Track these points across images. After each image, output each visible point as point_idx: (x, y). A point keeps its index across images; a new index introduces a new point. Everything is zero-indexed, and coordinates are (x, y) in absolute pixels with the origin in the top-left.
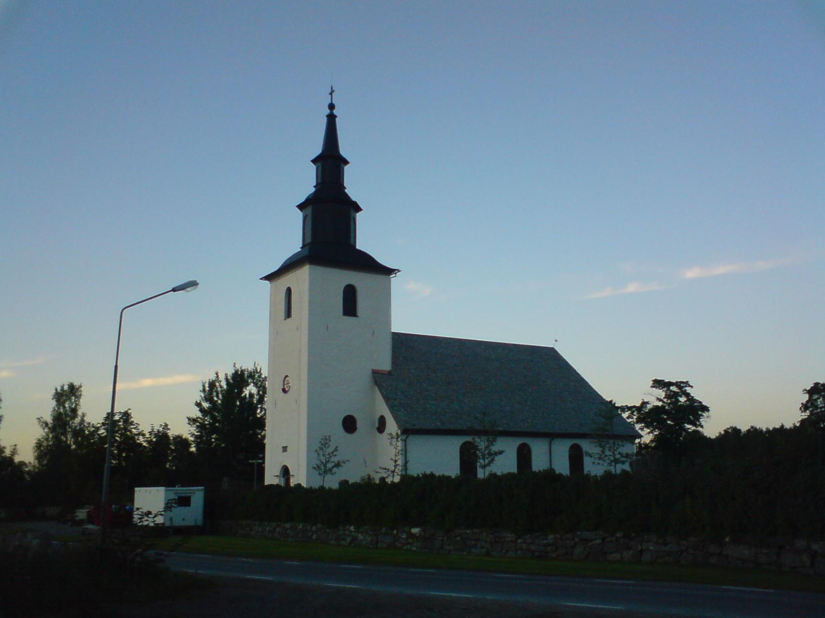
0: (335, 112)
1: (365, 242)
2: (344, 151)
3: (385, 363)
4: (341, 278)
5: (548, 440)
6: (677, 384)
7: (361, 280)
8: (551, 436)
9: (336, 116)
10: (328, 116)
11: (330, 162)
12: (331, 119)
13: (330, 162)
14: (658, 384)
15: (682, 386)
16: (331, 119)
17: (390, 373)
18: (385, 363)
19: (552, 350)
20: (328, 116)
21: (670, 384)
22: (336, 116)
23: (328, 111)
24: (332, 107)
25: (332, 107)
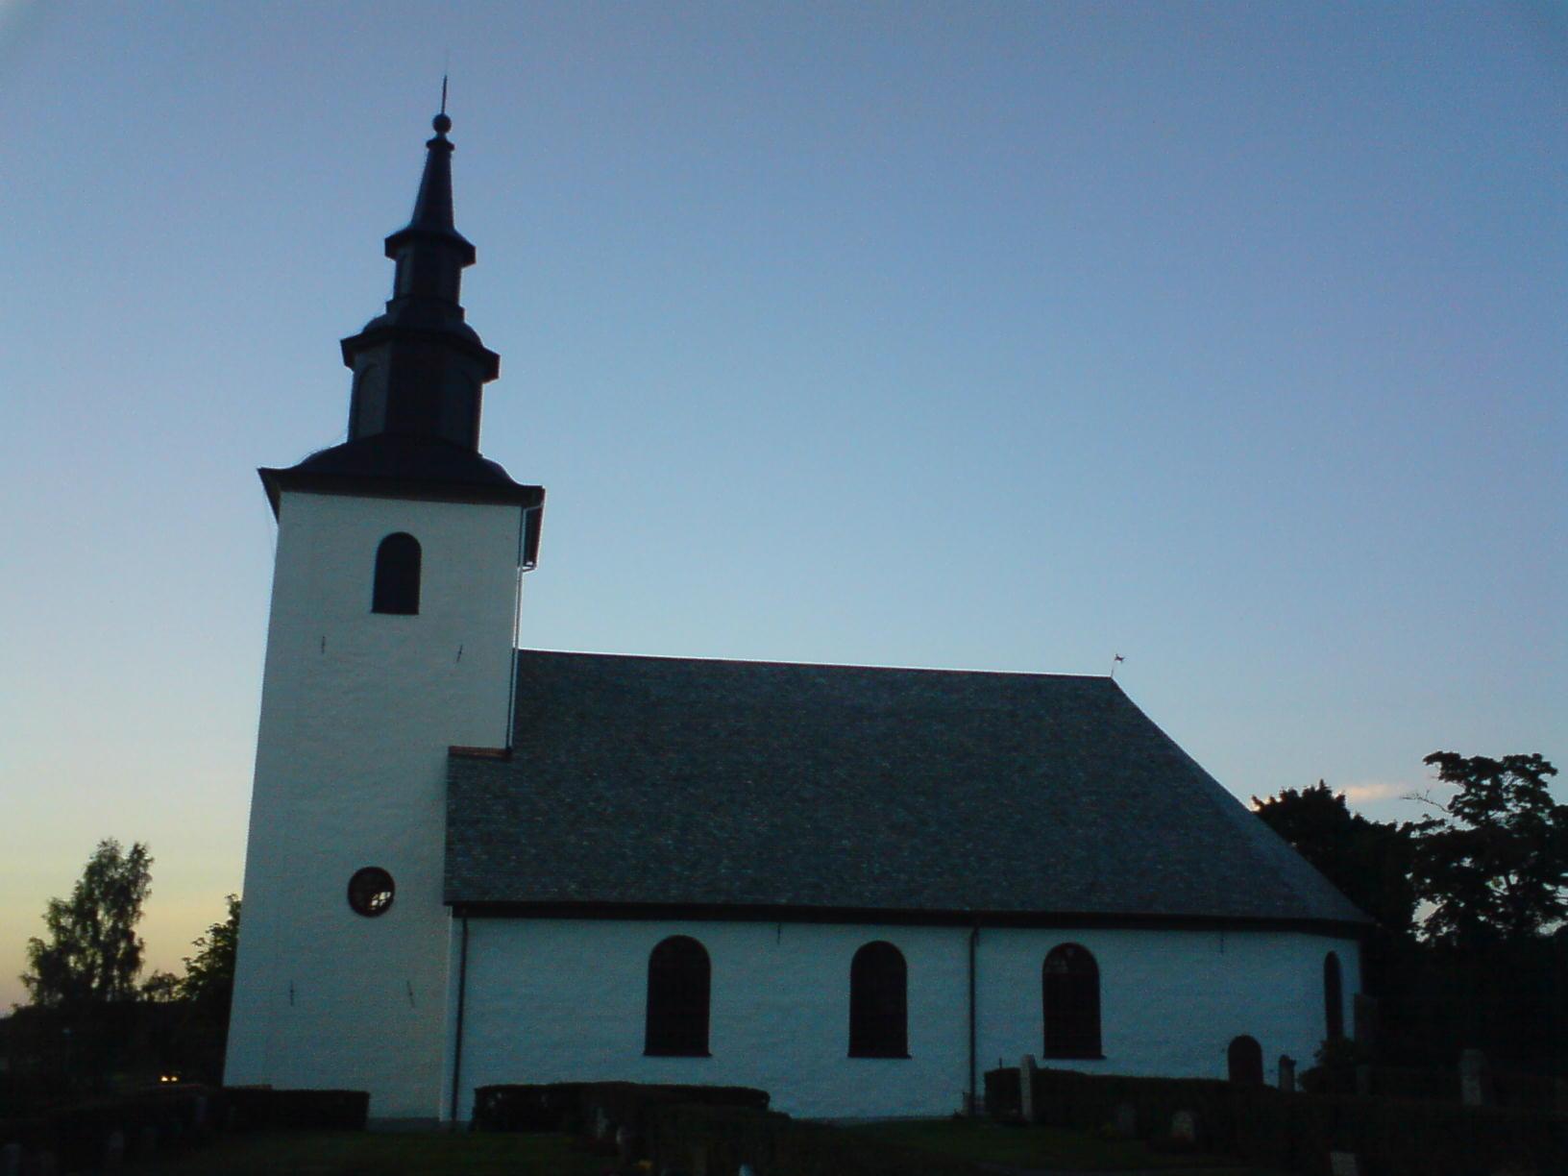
0: (450, 136)
1: (507, 432)
2: (465, 222)
3: (491, 730)
4: (366, 522)
5: (968, 932)
6: (1516, 764)
7: (434, 525)
8: (976, 921)
9: (451, 147)
10: (430, 144)
11: (430, 250)
12: (439, 152)
13: (430, 250)
14: (1452, 766)
15: (1532, 768)
16: (439, 152)
17: (506, 754)
18: (491, 730)
19: (1107, 686)
20: (430, 144)
21: (1483, 766)
22: (451, 147)
23: (433, 134)
24: (442, 123)
25: (442, 123)
